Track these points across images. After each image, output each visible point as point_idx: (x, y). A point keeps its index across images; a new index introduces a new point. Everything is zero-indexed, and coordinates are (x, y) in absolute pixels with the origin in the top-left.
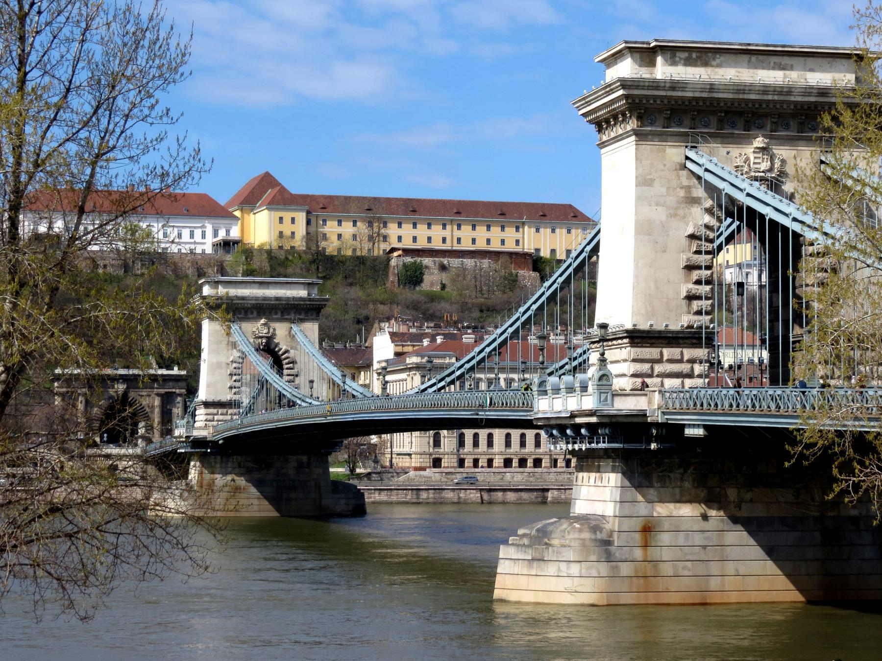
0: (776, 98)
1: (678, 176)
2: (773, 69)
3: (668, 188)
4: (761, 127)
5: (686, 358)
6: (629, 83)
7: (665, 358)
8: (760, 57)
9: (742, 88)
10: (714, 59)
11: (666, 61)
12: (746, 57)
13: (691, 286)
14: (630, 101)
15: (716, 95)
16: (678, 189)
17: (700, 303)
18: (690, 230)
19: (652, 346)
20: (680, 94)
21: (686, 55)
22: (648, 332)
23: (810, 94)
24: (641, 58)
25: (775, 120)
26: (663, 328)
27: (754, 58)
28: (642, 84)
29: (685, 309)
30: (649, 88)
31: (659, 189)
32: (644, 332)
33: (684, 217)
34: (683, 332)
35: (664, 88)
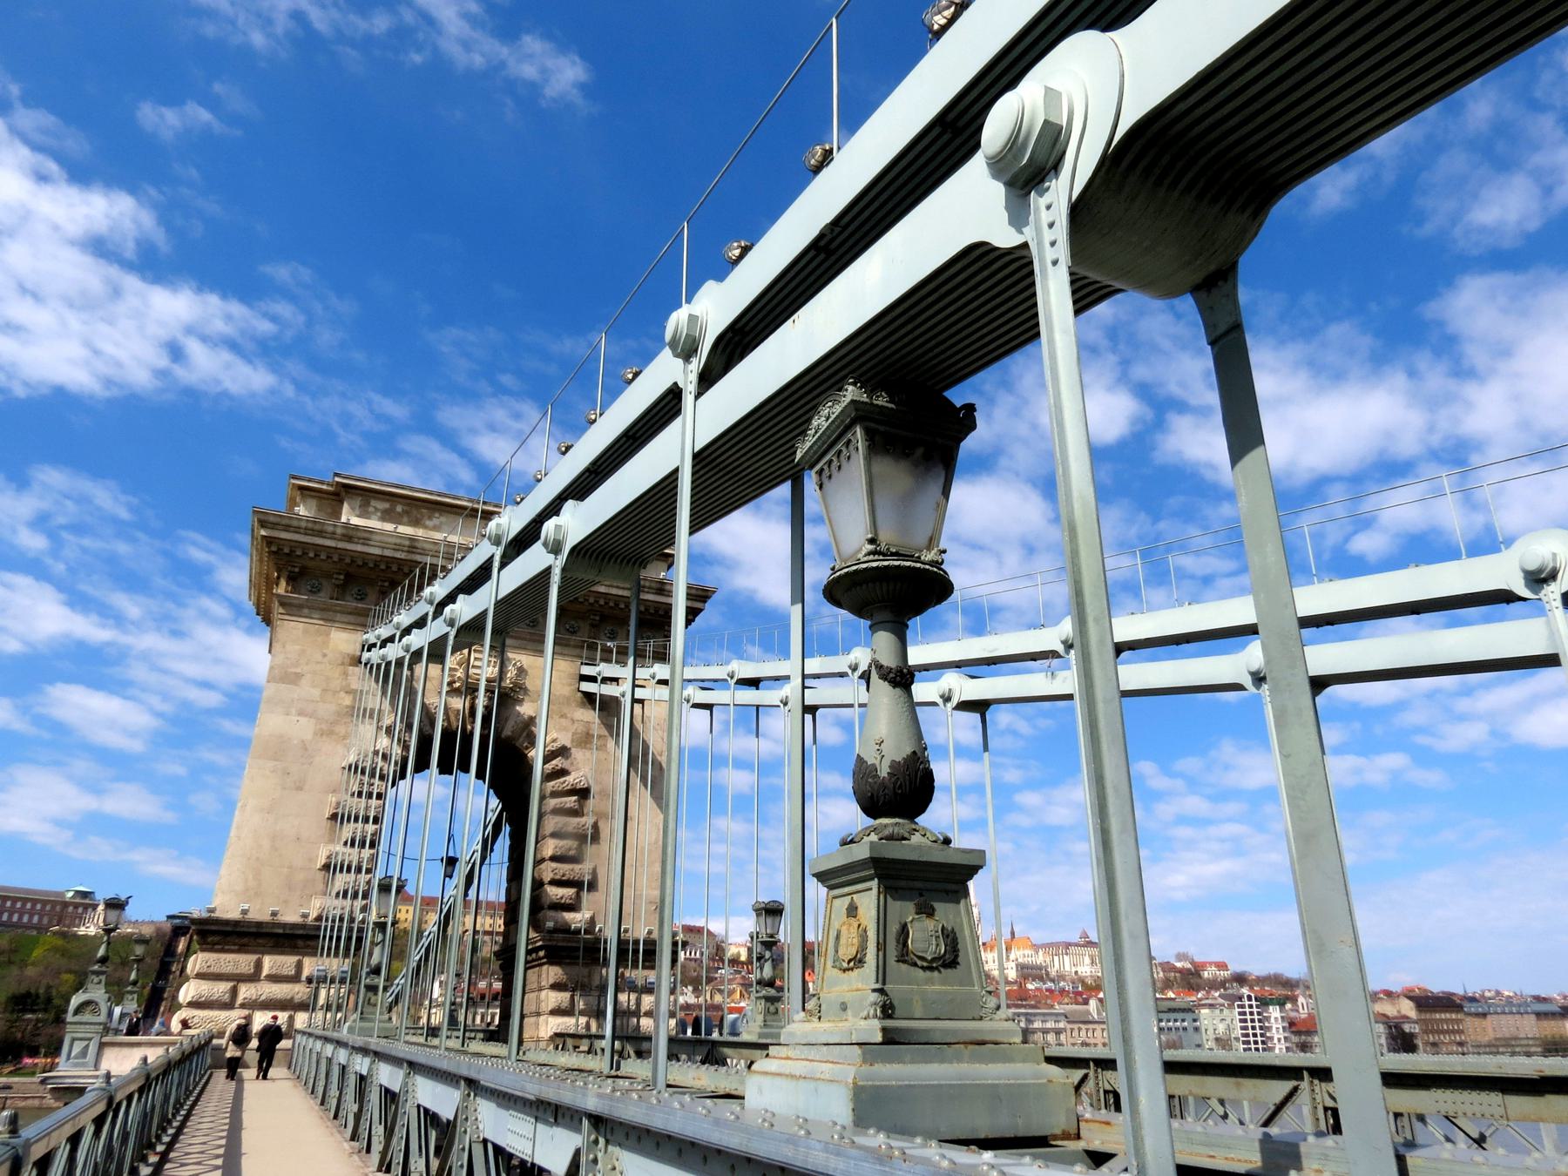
1: (346, 674)
3: (325, 690)
5: (306, 973)
6: (272, 519)
7: (265, 972)
10: (430, 518)
11: (353, 509)
13: (339, 848)
14: (274, 548)
16: (342, 694)
18: (352, 759)
19: (242, 949)
20: (359, 548)
21: (387, 505)
22: (236, 923)
26: (265, 917)
29: (321, 886)
31: (307, 690)
32: (227, 922)
33: (344, 738)
34: (303, 926)
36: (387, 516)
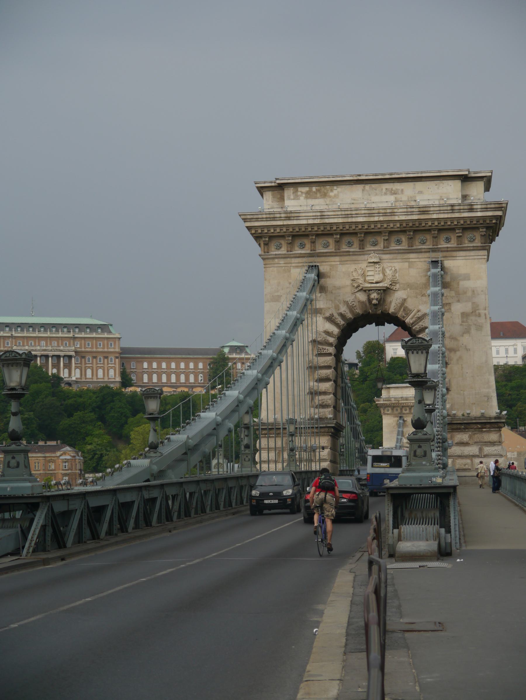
0: (381, 219)
2: (386, 194)
4: (375, 244)
8: (374, 186)
9: (349, 212)
10: (332, 191)
12: (360, 187)
14: (253, 232)
15: (327, 221)
17: (321, 397)
20: (295, 222)
23: (412, 213)
24: (273, 195)
25: (386, 238)
27: (367, 187)
28: (260, 216)
30: (267, 219)
35: (280, 219)
36: (308, 195)
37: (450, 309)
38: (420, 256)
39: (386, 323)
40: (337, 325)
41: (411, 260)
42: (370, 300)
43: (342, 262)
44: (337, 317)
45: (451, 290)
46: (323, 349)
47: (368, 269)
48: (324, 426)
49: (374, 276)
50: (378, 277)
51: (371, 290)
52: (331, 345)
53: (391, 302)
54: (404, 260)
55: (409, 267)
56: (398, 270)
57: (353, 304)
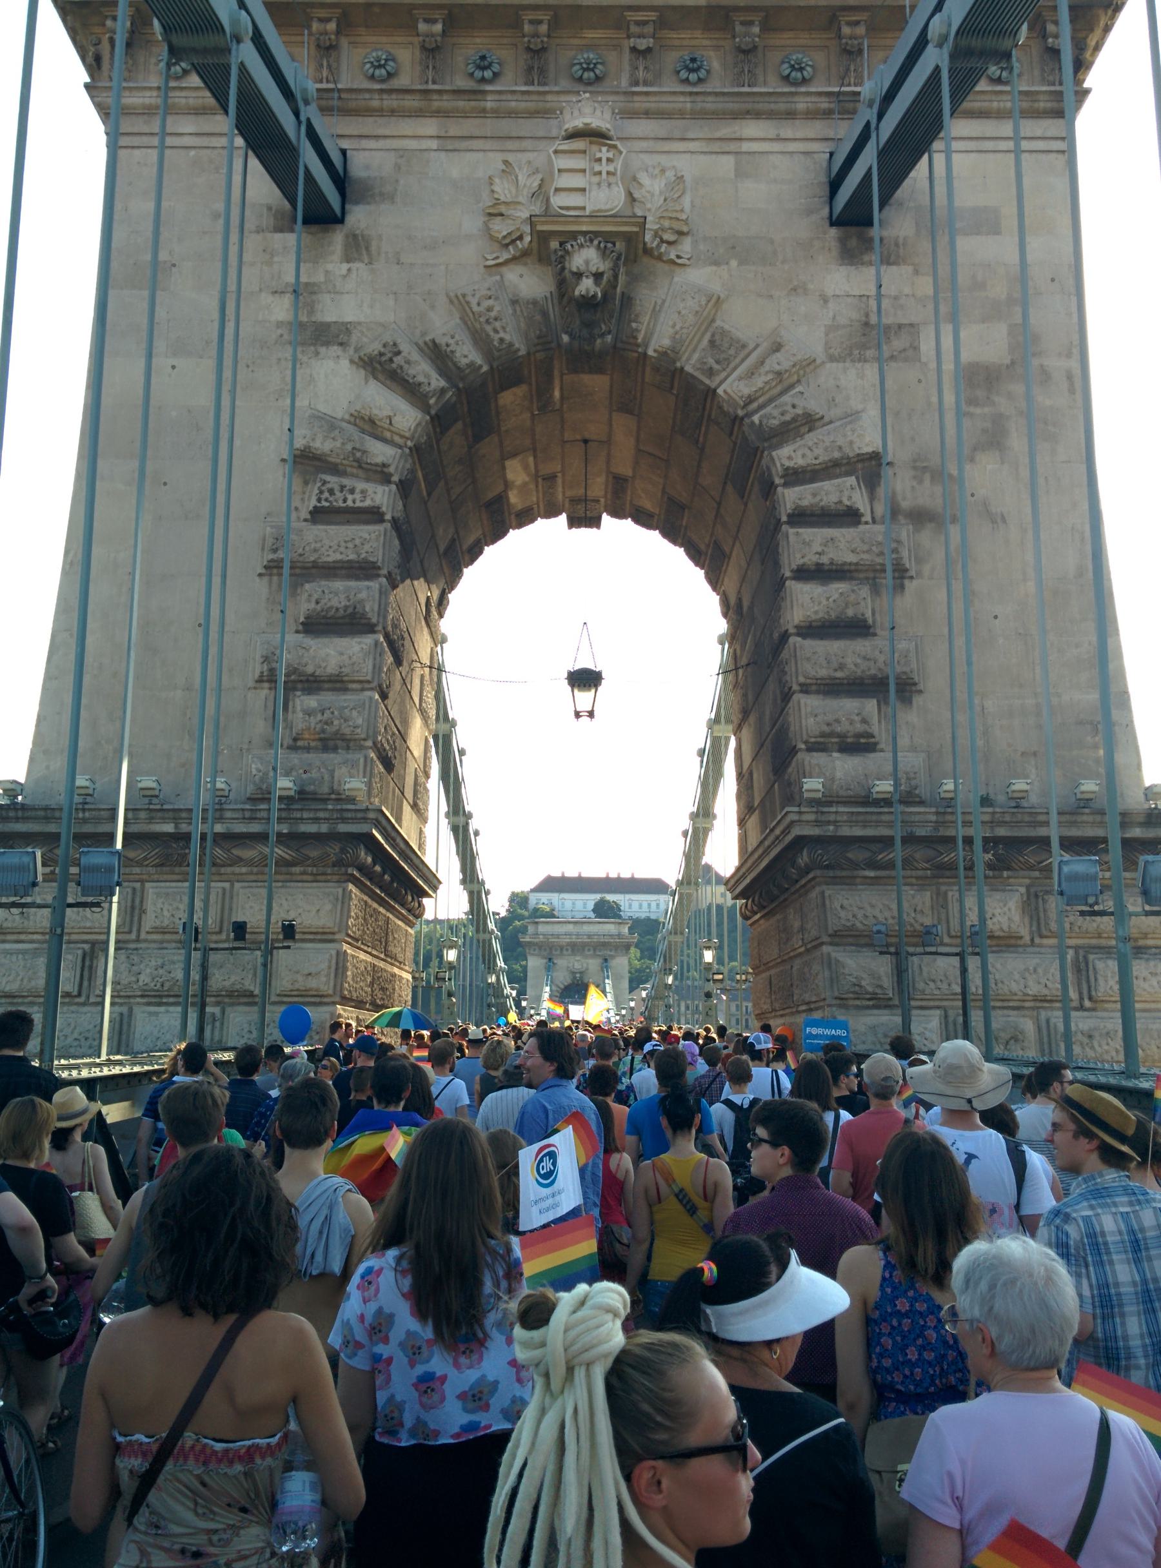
25: (642, 44)
37: (916, 349)
38: (788, 133)
39: (605, 518)
40: (411, 390)
41: (746, 146)
42: (564, 282)
43: (448, 143)
44: (415, 356)
45: (916, 272)
46: (342, 488)
47: (562, 162)
48: (324, 828)
49: (588, 191)
50: (607, 199)
51: (574, 235)
52: (381, 474)
53: (656, 313)
54: (716, 147)
55: (740, 173)
56: (688, 178)
57: (489, 309)
